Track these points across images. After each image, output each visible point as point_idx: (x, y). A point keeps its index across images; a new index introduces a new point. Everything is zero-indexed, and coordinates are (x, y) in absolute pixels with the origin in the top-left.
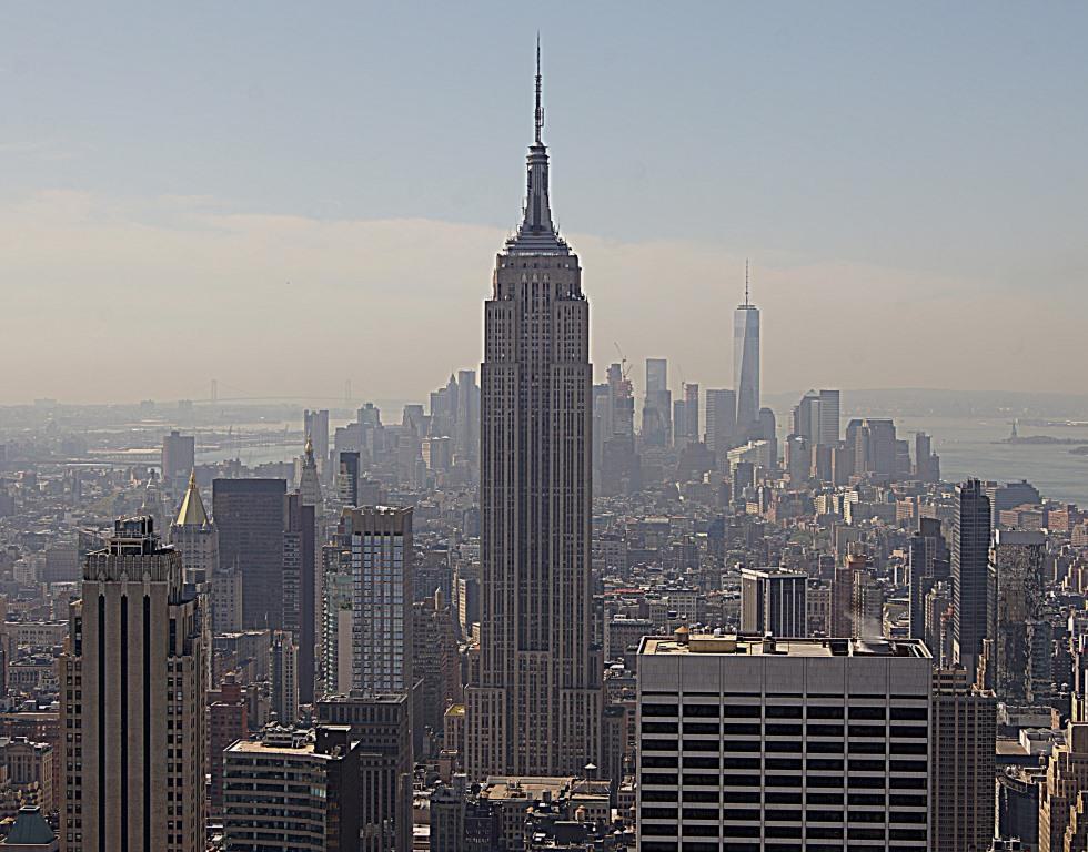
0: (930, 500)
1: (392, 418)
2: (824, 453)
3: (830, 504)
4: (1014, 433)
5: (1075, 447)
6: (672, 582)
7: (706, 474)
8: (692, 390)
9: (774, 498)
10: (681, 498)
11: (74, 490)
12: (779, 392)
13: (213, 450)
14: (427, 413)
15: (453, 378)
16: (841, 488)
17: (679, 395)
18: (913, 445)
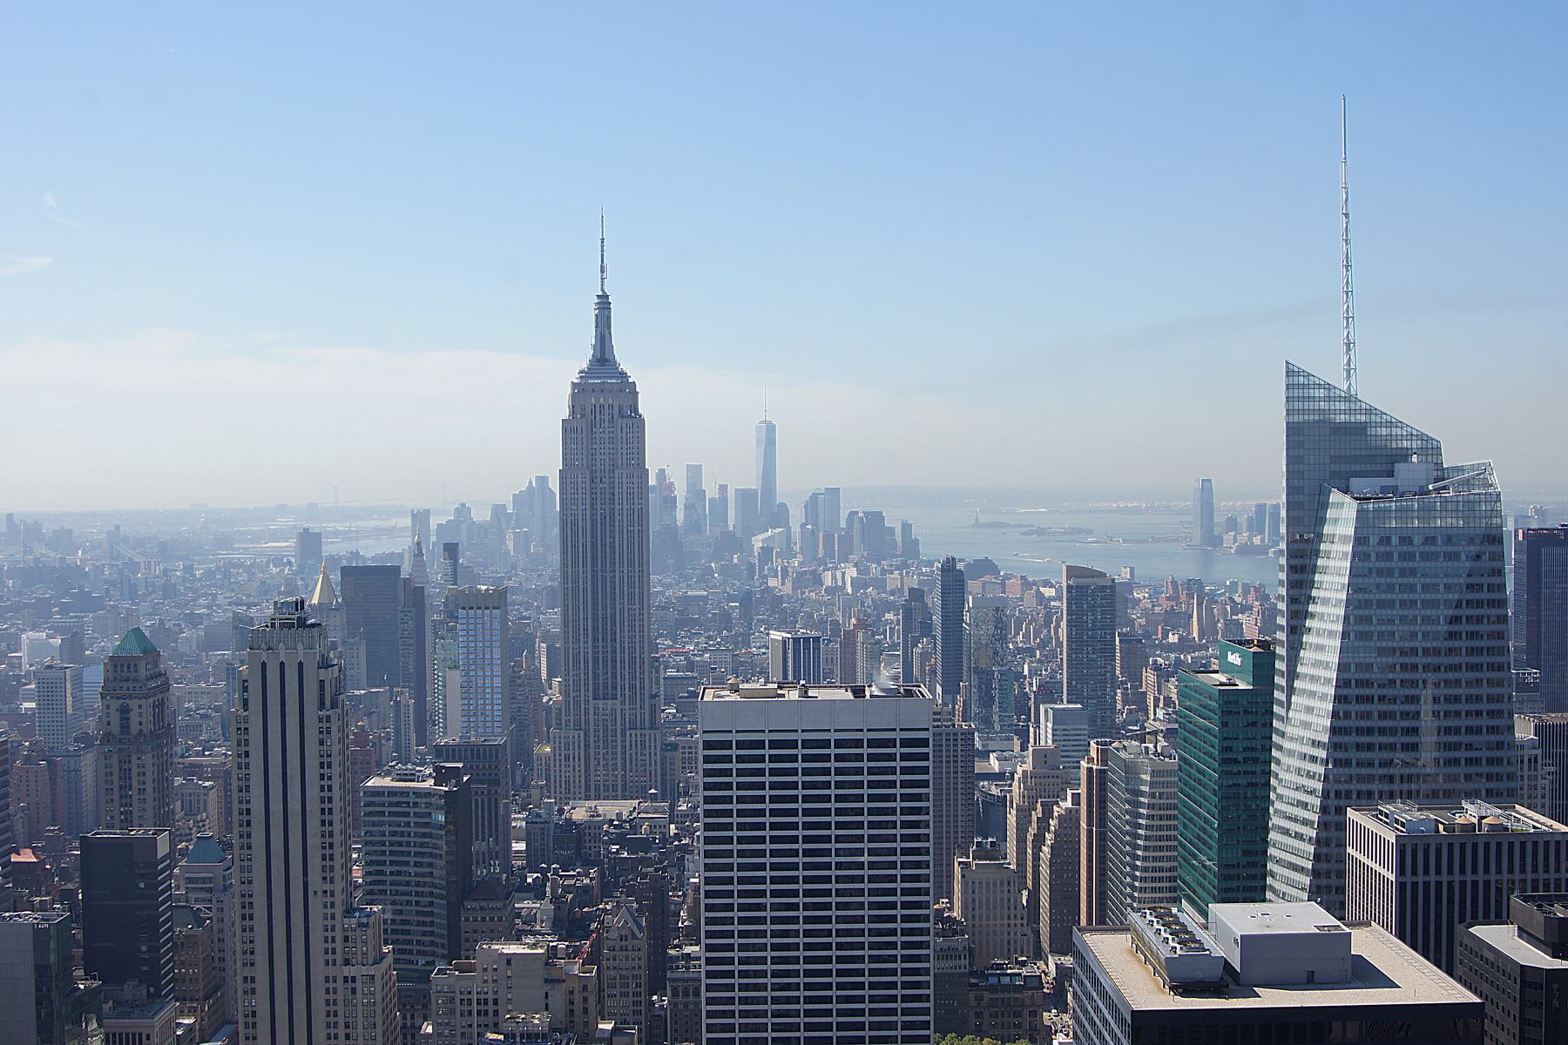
0: (913, 574)
1: (481, 515)
2: (828, 539)
3: (834, 578)
4: (977, 519)
5: (1025, 530)
6: (711, 643)
7: (736, 556)
8: (723, 488)
9: (790, 574)
10: (716, 575)
11: (225, 577)
12: (793, 487)
13: (337, 542)
14: (510, 511)
15: (530, 482)
16: (843, 565)
17: (711, 492)
18: (898, 531)
